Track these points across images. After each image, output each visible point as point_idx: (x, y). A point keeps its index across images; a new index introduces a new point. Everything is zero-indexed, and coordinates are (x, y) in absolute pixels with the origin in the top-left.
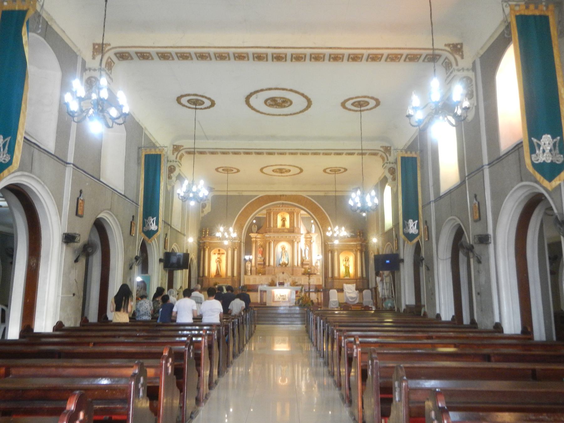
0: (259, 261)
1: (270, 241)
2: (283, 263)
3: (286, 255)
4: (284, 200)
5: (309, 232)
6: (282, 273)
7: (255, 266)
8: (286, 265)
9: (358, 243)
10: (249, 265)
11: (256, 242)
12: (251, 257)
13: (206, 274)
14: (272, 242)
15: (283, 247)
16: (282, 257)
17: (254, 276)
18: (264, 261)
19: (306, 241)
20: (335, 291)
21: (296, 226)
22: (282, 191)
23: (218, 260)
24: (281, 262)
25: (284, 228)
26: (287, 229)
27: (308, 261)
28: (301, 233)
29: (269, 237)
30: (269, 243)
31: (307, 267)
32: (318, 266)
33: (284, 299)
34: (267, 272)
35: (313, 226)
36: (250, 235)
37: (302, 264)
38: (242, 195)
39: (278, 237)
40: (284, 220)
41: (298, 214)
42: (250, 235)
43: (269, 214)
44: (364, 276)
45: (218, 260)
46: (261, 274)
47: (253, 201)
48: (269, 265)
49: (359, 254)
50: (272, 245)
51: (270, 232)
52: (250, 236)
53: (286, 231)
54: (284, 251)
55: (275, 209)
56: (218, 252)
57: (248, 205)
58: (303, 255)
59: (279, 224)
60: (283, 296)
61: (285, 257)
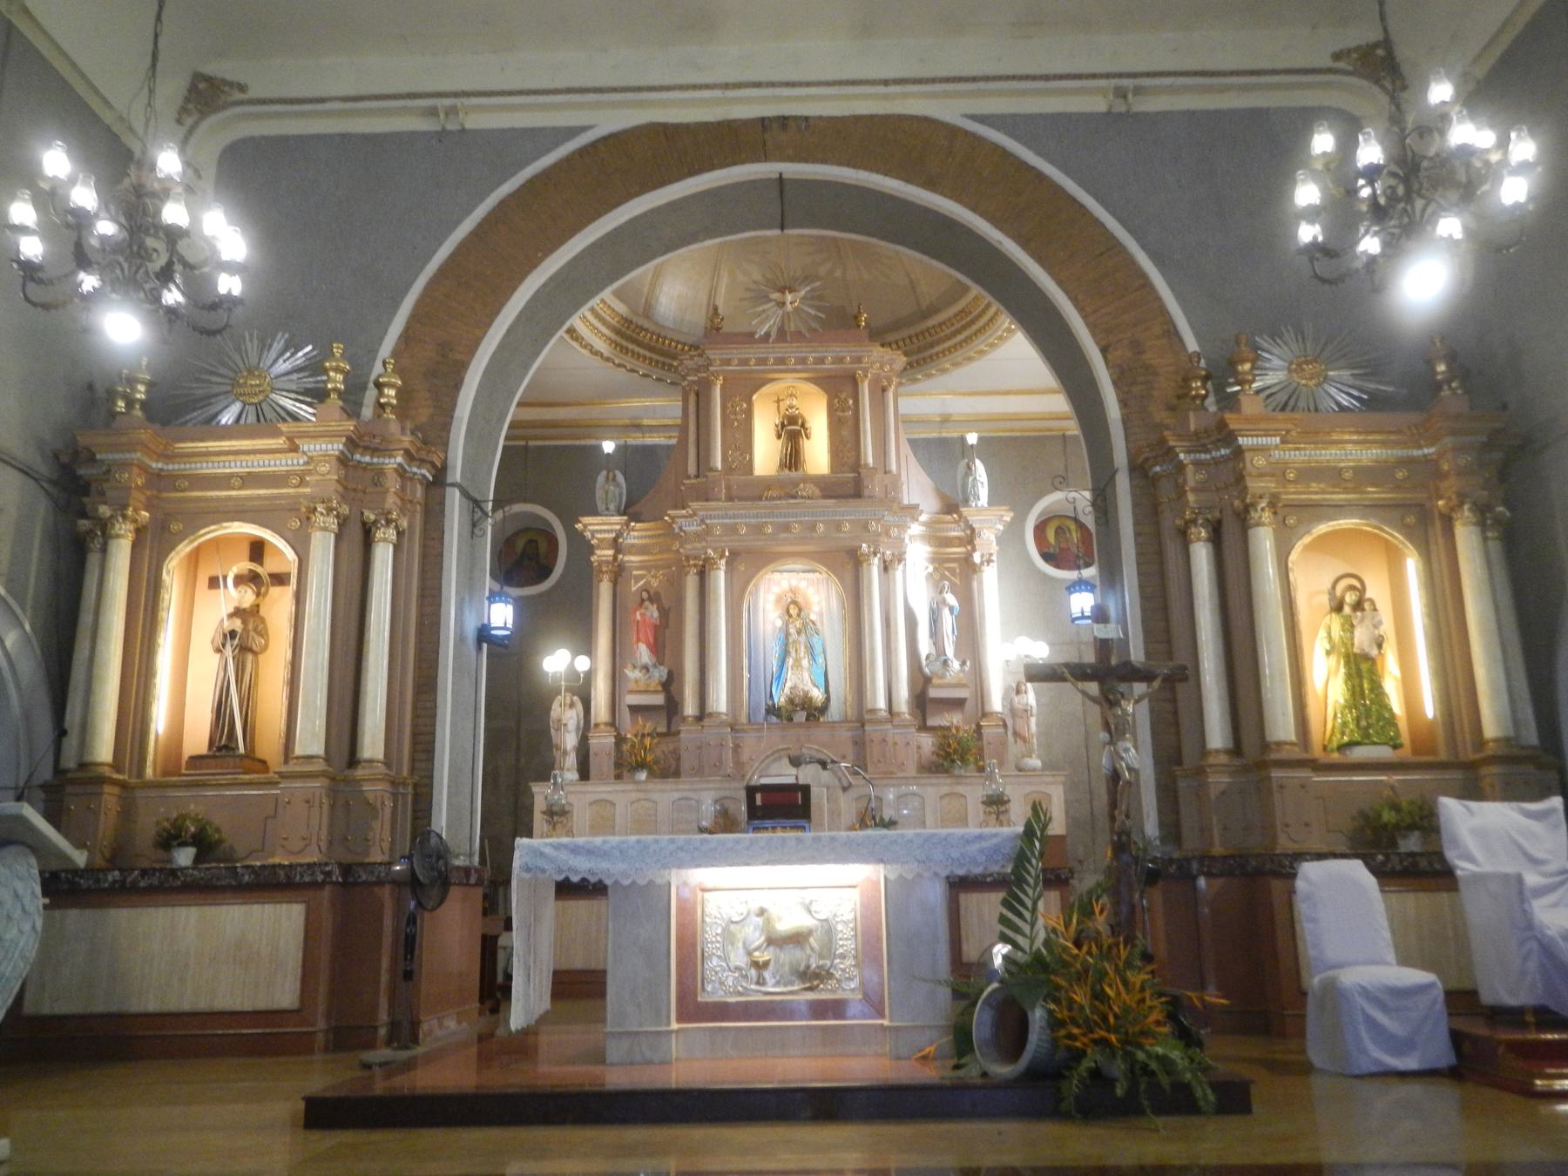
0: (631, 692)
1: (707, 559)
2: (791, 701)
3: (811, 650)
4: (782, 160)
5: (952, 505)
6: (786, 761)
7: (612, 724)
8: (814, 712)
9: (1448, 441)
10: (566, 718)
11: (619, 573)
12: (583, 663)
13: (104, 749)
14: (723, 562)
15: (794, 602)
16: (790, 661)
17: (599, 789)
18: (671, 686)
19: (938, 560)
20: (1356, 869)
21: (870, 461)
22: (772, 85)
23: (227, 625)
24: (780, 699)
25: (793, 474)
26: (818, 481)
27: (964, 686)
28: (906, 502)
29: (699, 536)
30: (702, 575)
31: (953, 719)
32: (1026, 711)
33: (811, 977)
34: (686, 764)
35: (980, 468)
36: (579, 526)
37: (921, 702)
38: (463, 131)
39: (758, 529)
40: (792, 431)
41: (884, 390)
42: (579, 526)
43: (697, 395)
44: (1531, 736)
45: (237, 624)
46: (643, 776)
47: (546, 175)
48: (702, 715)
49: (1467, 538)
50: (720, 578)
51: (707, 500)
52: (580, 535)
53: (811, 489)
54: (798, 624)
55: (735, 353)
56: (244, 566)
57: (503, 204)
58: (925, 647)
59: (765, 453)
60: (797, 939)
61: (805, 663)
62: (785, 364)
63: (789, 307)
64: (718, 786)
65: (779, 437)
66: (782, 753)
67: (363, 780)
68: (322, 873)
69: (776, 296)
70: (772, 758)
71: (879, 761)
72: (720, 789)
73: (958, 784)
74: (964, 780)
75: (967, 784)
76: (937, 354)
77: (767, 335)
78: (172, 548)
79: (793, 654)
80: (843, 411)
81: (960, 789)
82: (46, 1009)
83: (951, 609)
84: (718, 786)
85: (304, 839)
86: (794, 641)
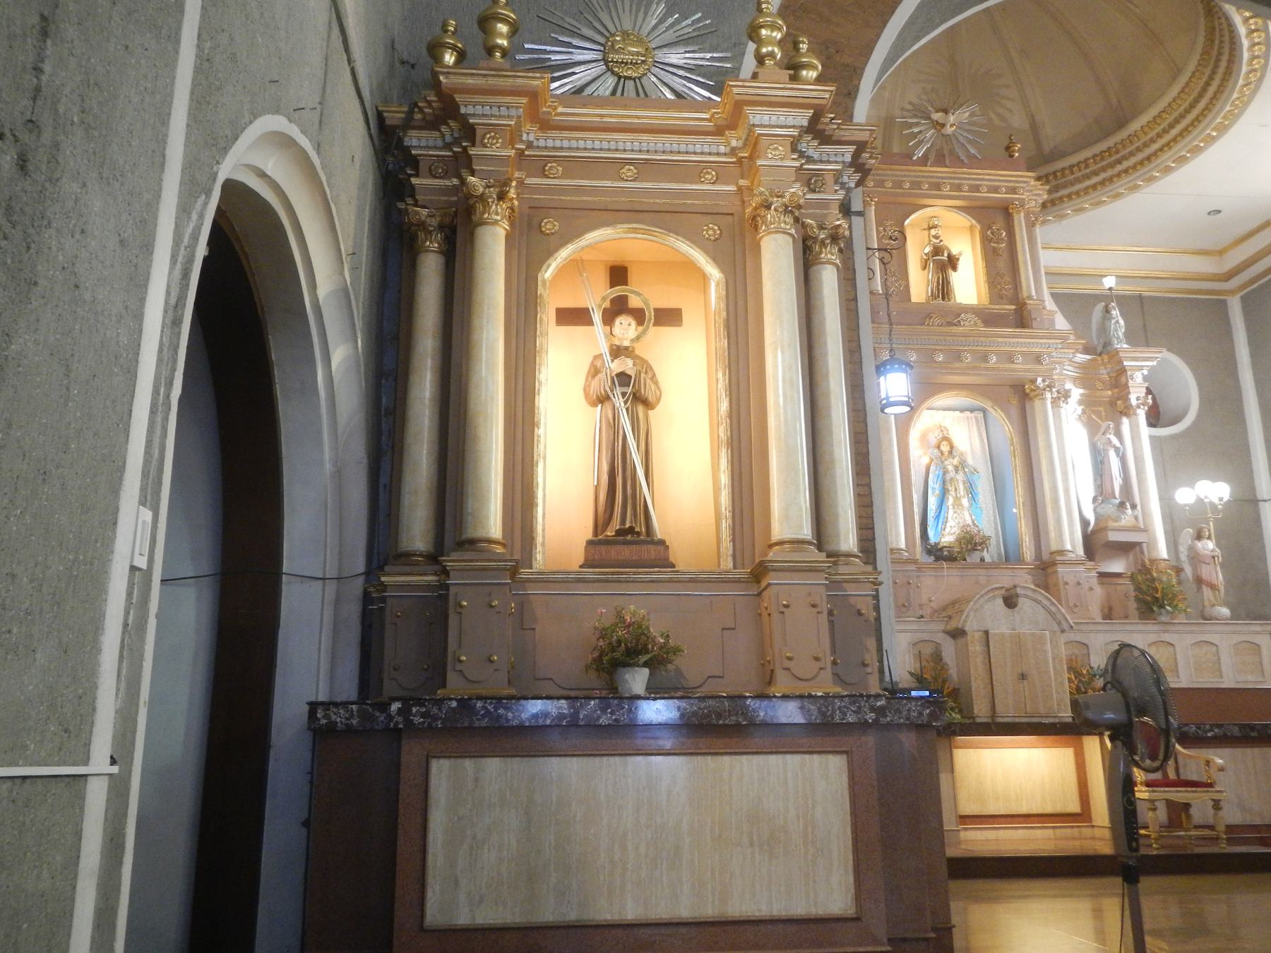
6: (1000, 601)
15: (946, 439)
16: (951, 501)
62: (939, 189)
63: (949, 130)
64: (915, 627)
65: (924, 268)
66: (996, 592)
67: (847, 581)
68: (873, 709)
69: (937, 116)
70: (986, 597)
71: (1076, 606)
72: (915, 631)
73: (1165, 631)
74: (1168, 628)
75: (1175, 632)
76: (1061, 198)
77: (925, 156)
78: (550, 253)
79: (953, 493)
80: (998, 243)
81: (1167, 637)
82: (463, 919)
84: (915, 627)
85: (817, 659)
86: (951, 479)
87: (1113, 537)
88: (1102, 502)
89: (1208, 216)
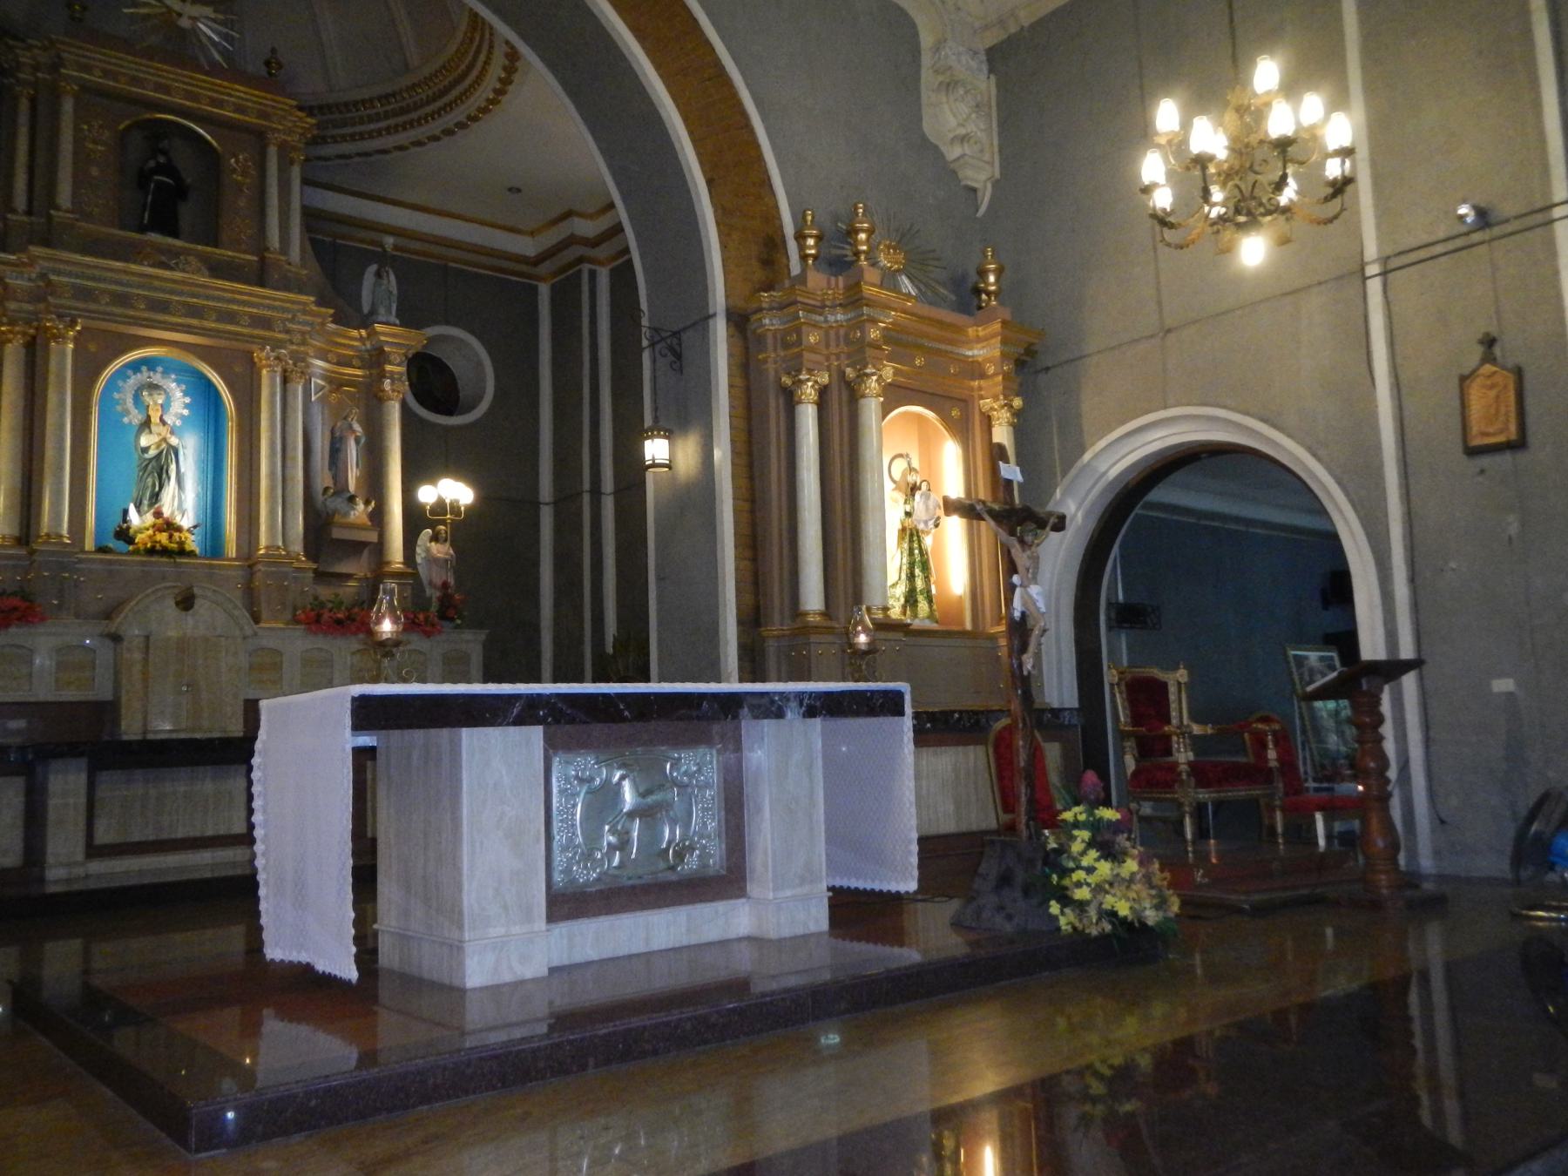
6: (172, 603)
58: (323, 479)
83: (357, 441)
87: (337, 533)
88: (335, 494)
89: (508, 193)
